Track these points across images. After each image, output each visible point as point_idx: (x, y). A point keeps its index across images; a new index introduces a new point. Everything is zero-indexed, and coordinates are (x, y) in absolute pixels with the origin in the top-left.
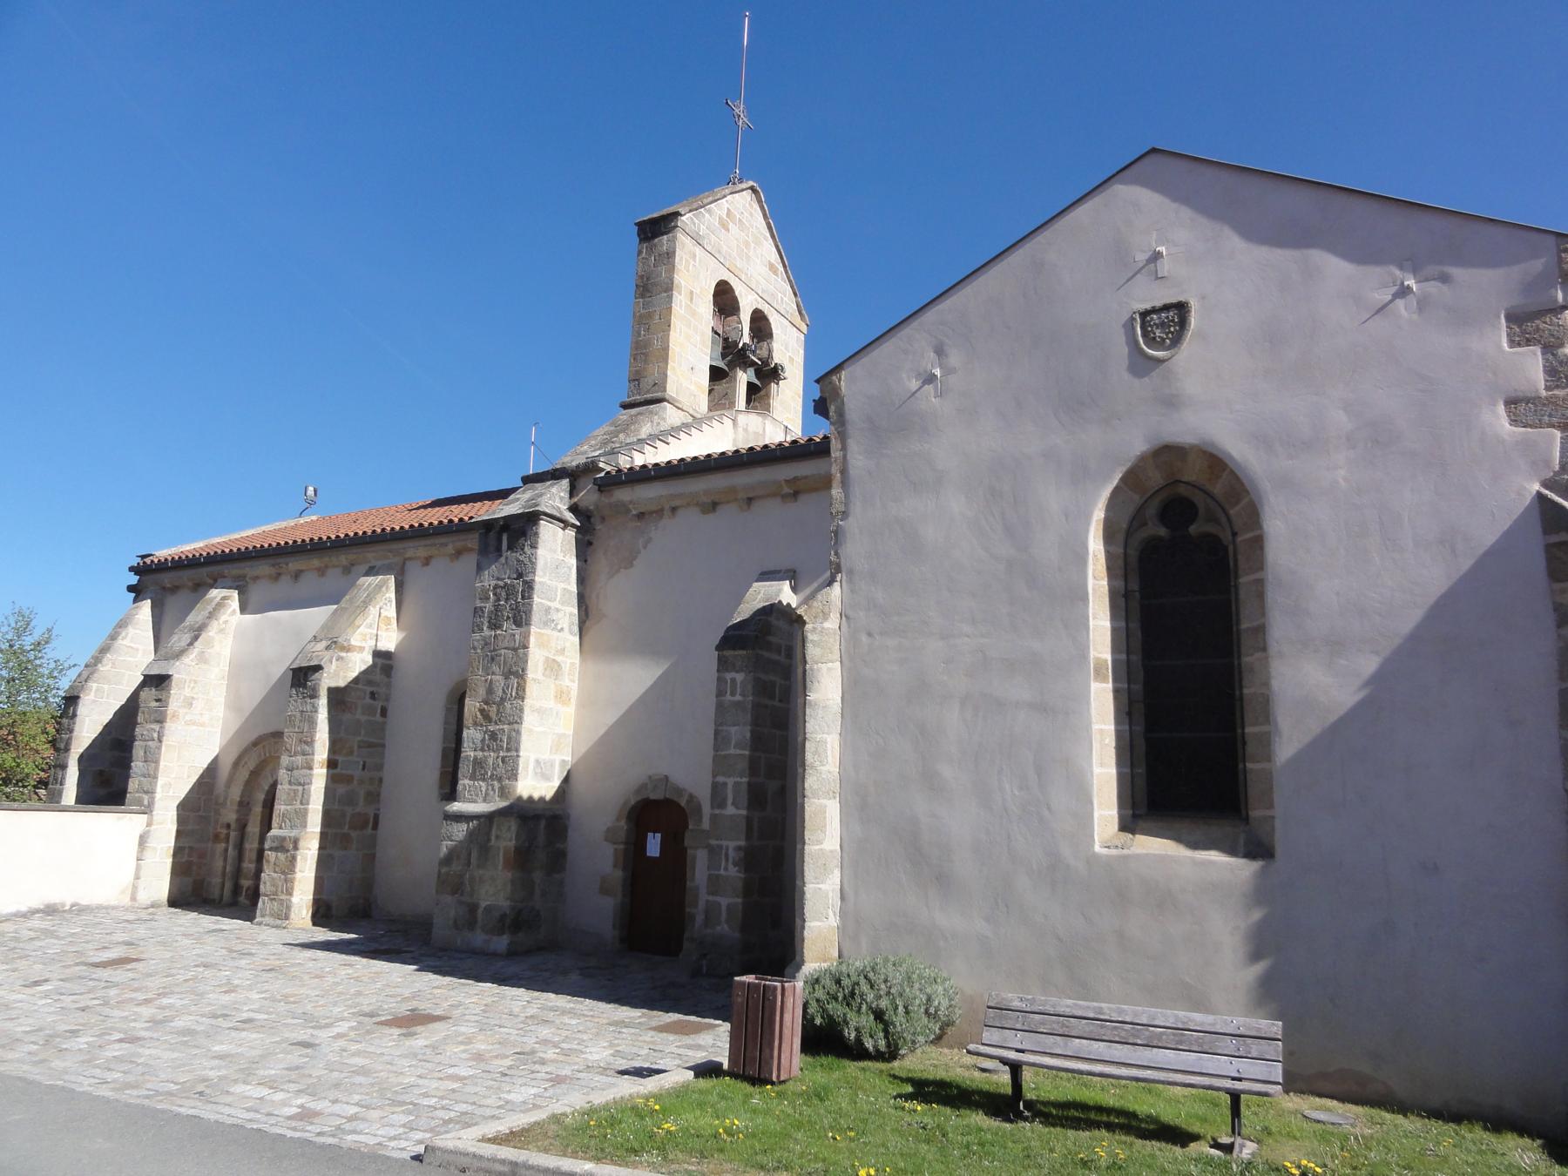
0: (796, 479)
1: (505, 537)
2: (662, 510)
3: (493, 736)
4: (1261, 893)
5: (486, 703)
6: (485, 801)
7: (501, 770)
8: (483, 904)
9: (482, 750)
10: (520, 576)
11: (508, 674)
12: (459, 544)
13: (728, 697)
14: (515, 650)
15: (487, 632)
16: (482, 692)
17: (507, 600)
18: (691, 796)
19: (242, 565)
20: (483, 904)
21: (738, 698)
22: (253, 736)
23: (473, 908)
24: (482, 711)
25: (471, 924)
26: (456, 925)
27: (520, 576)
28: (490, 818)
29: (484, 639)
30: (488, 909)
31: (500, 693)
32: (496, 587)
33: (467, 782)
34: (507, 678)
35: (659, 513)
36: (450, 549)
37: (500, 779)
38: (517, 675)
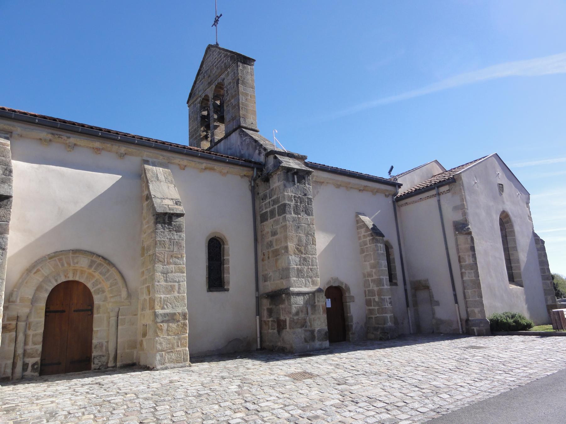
0: (367, 186)
1: (295, 177)
2: (323, 182)
3: (305, 259)
4: (526, 293)
5: (298, 245)
6: (305, 287)
7: (311, 274)
8: (317, 329)
9: (300, 265)
10: (305, 195)
11: (307, 234)
12: (209, 165)
13: (380, 251)
14: (309, 225)
15: (293, 215)
16: (295, 240)
17: (301, 203)
18: (346, 284)
19: (15, 124)
20: (317, 329)
21: (382, 252)
22: (50, 250)
23: (312, 332)
24: (297, 249)
25: (313, 338)
26: (306, 341)
27: (305, 195)
28: (313, 293)
29: (293, 218)
30: (319, 331)
31: (305, 241)
32: (295, 197)
33: (295, 279)
34: (306, 236)
35: (322, 183)
36: (204, 165)
37: (311, 277)
38: (311, 235)
